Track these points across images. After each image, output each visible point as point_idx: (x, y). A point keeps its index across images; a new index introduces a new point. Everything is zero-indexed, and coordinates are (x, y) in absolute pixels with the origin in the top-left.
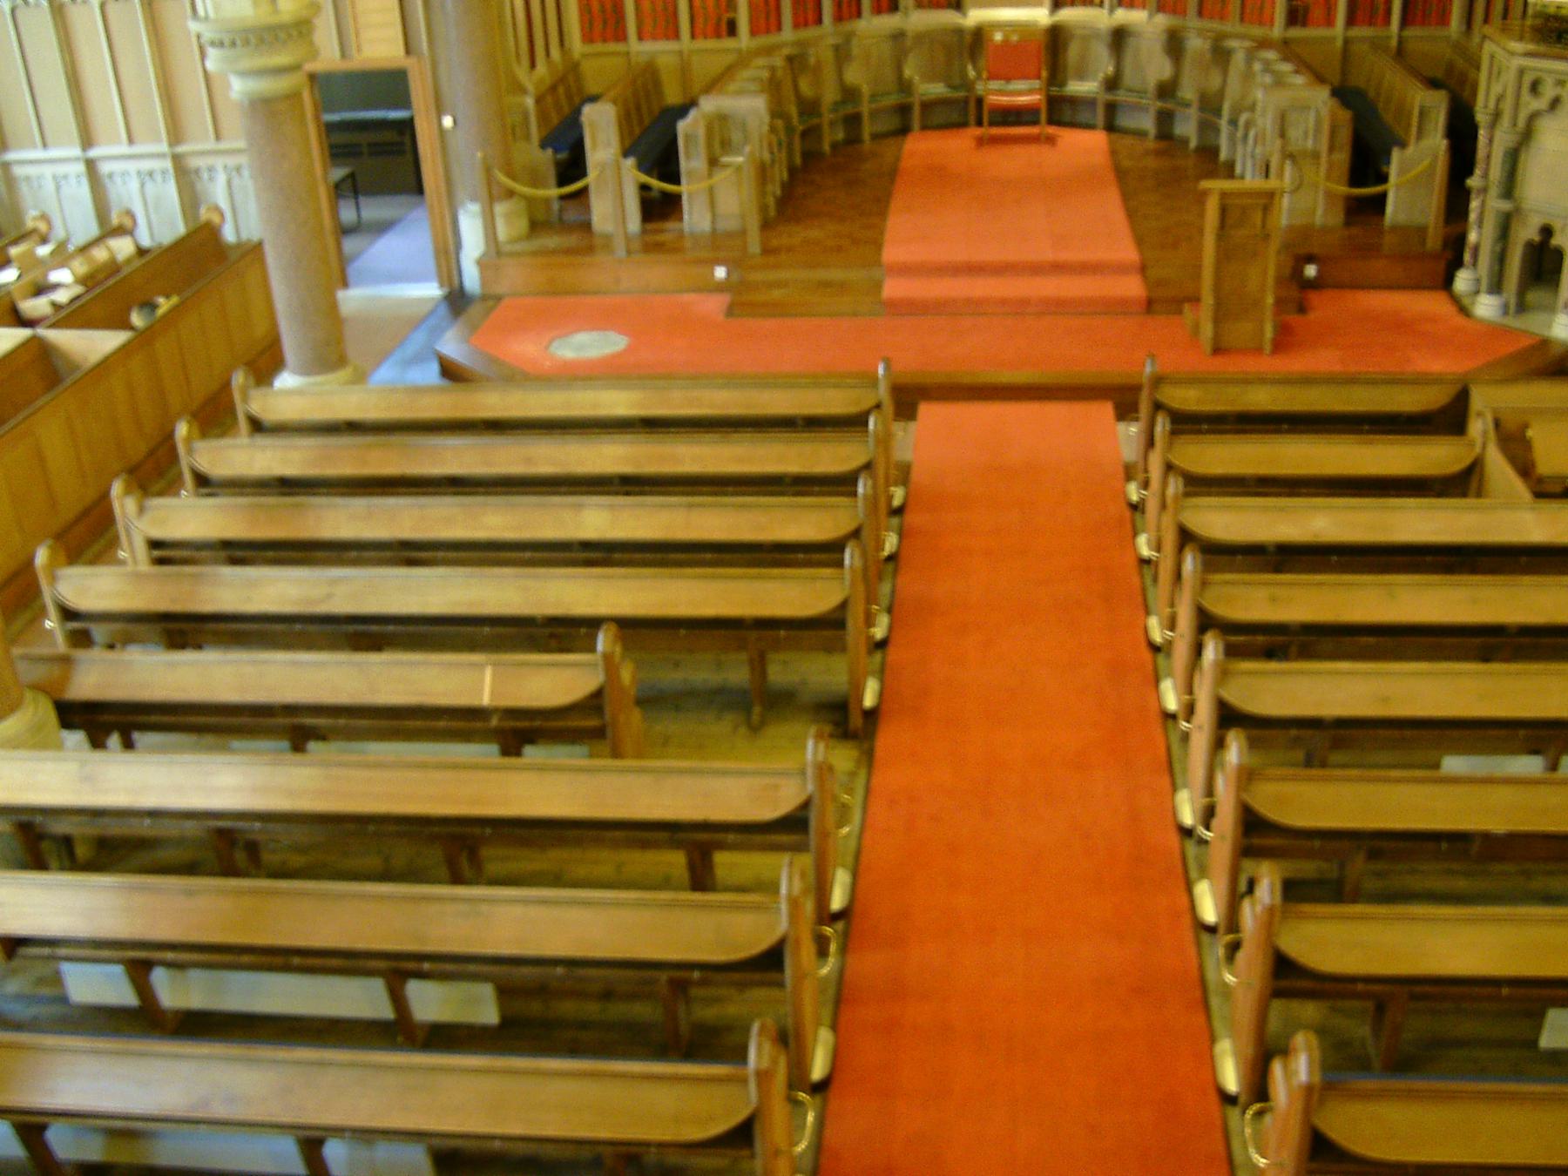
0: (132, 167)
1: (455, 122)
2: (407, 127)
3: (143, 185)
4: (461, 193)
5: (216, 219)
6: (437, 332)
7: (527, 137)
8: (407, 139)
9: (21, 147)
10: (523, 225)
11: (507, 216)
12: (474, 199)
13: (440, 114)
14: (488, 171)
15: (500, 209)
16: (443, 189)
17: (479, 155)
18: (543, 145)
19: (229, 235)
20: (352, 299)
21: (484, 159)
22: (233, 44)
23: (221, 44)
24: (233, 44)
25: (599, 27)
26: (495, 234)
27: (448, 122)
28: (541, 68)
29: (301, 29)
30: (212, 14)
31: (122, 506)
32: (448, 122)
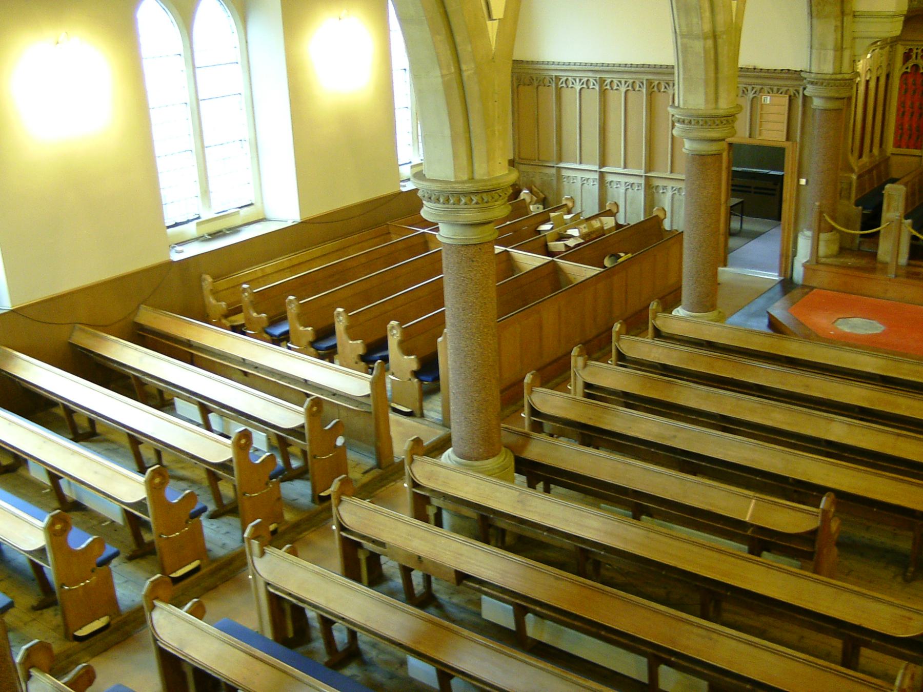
0: (623, 179)
1: (807, 182)
2: (780, 179)
3: (626, 190)
4: (802, 224)
5: (661, 215)
6: (772, 301)
7: (849, 198)
8: (778, 187)
9: (567, 162)
10: (835, 248)
11: (827, 241)
12: (809, 229)
13: (799, 177)
14: (821, 213)
15: (823, 236)
16: (793, 220)
17: (817, 204)
18: (857, 204)
19: (667, 225)
20: (726, 273)
21: (820, 206)
22: (690, 122)
23: (683, 122)
24: (690, 122)
25: (906, 137)
26: (817, 252)
27: (803, 182)
28: (865, 159)
29: (729, 119)
30: (681, 106)
31: (576, 362)
32: (803, 182)
